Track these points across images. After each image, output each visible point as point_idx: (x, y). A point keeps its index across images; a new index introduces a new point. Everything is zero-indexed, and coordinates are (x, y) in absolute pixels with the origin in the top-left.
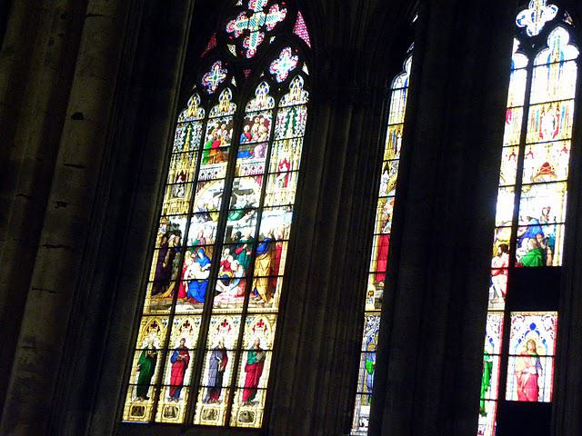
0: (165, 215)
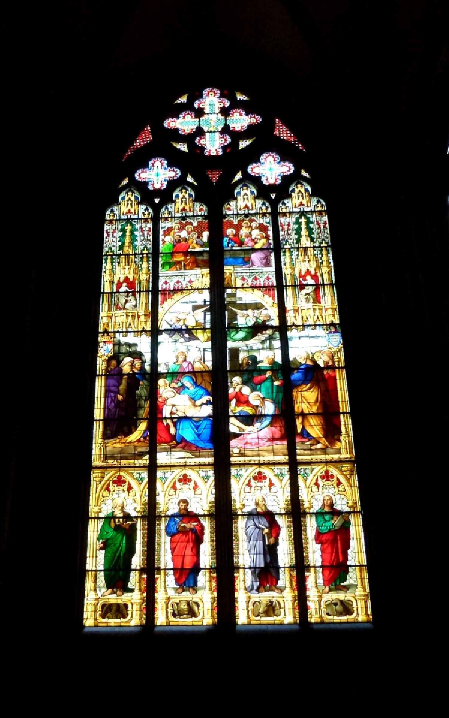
0: (106, 332)
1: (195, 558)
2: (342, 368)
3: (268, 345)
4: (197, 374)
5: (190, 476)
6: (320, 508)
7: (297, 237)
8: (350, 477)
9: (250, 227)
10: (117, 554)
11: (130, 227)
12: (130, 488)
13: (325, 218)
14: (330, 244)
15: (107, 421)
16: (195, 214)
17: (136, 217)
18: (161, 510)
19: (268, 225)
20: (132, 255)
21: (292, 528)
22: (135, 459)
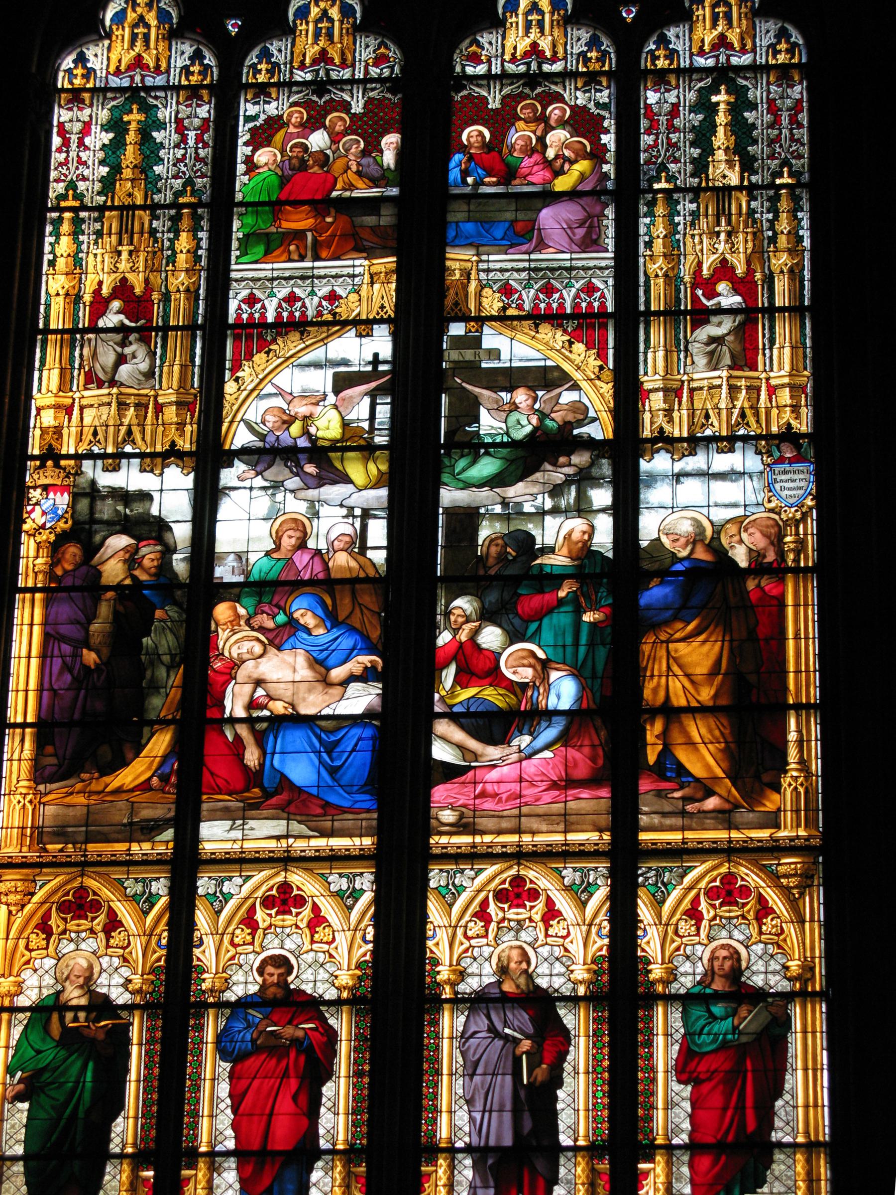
0: (51, 455)
1: (305, 1122)
2: (806, 569)
3: (572, 501)
4: (338, 587)
5: (299, 889)
6: (699, 983)
7: (696, 152)
8: (802, 895)
9: (543, 119)
10: (68, 1111)
11: (141, 117)
12: (113, 924)
13: (798, 91)
14: (806, 177)
15: (45, 730)
16: (359, 75)
17: (160, 81)
18: (204, 986)
19: (603, 113)
20: (143, 208)
21: (606, 1039)
22: (130, 841)
